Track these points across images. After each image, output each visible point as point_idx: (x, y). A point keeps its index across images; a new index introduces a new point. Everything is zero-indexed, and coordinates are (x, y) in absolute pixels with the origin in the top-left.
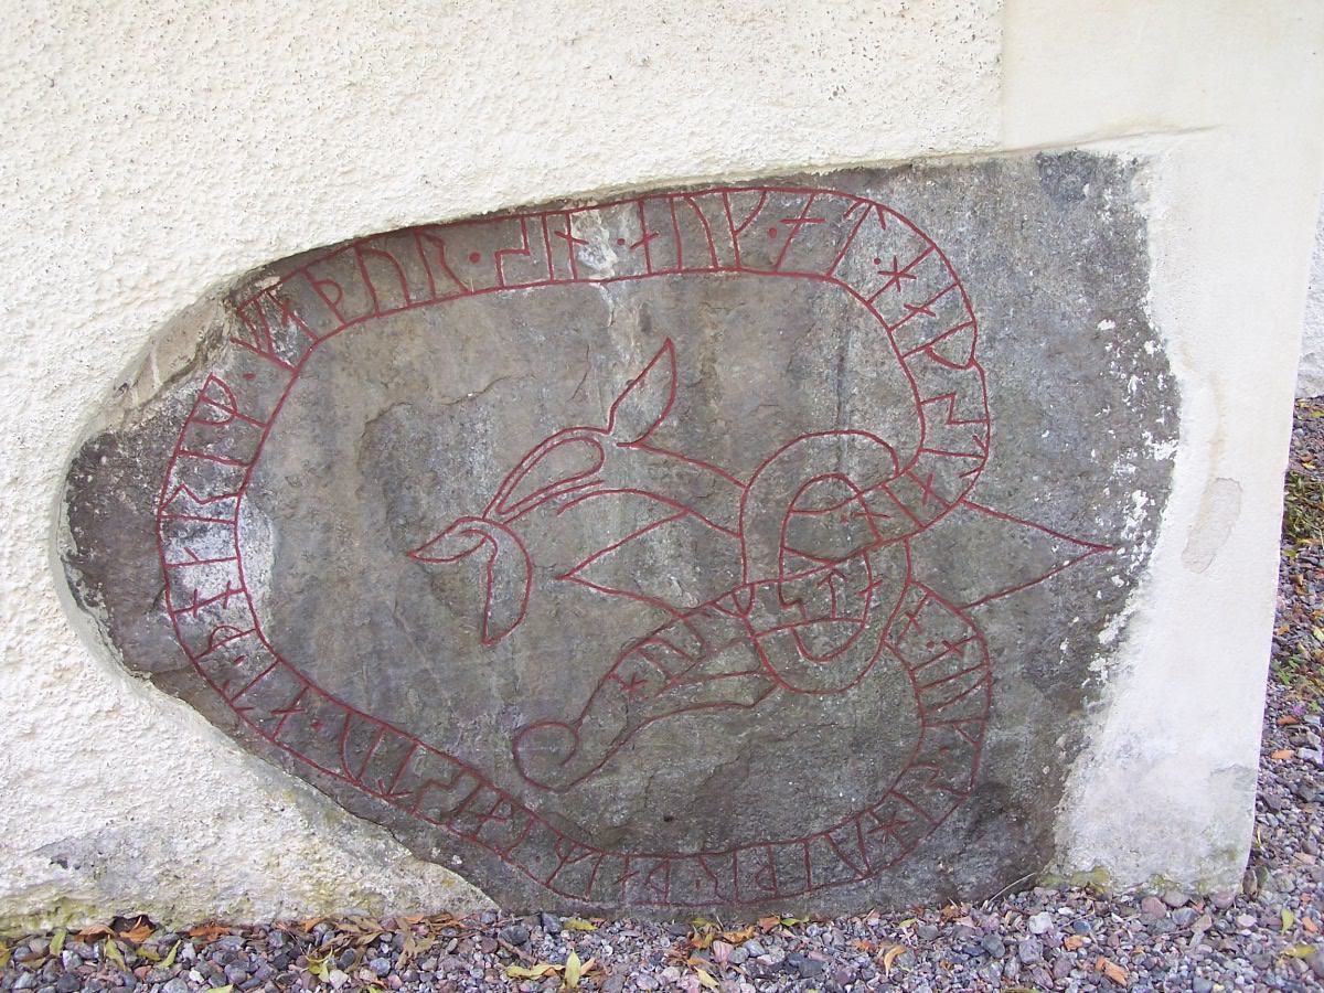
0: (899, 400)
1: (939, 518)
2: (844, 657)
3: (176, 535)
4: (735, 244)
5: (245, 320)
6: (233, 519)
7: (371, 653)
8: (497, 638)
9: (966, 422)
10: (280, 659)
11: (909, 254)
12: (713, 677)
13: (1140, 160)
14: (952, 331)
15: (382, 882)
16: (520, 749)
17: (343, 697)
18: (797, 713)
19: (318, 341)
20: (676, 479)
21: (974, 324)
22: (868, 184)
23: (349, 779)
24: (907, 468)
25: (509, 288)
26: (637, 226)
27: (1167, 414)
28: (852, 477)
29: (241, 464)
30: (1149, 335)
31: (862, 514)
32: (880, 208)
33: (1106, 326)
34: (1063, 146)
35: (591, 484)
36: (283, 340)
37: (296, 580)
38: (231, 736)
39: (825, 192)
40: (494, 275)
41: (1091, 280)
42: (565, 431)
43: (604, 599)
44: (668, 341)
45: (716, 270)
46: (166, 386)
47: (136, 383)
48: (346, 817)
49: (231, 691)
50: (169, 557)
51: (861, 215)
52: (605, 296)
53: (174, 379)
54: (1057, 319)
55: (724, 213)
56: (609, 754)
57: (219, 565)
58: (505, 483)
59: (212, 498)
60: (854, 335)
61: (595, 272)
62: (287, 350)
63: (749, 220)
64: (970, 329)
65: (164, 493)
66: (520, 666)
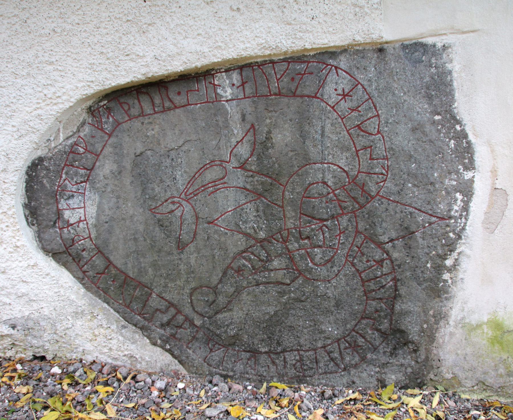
0: (348, 150)
1: (368, 203)
2: (329, 265)
3: (63, 198)
4: (278, 85)
5: (94, 116)
6: (83, 192)
7: (134, 251)
8: (183, 248)
9: (377, 159)
10: (99, 251)
11: (349, 87)
12: (272, 270)
13: (446, 45)
14: (369, 119)
15: (133, 349)
16: (193, 298)
17: (123, 269)
18: (308, 289)
19: (119, 124)
20: (256, 183)
21: (378, 116)
22: (331, 58)
23: (125, 306)
24: (354, 180)
25: (191, 105)
26: (239, 78)
27: (469, 158)
28: (330, 183)
29: (88, 170)
30: (459, 122)
31: (335, 200)
32: (336, 68)
33: (437, 118)
34: (411, 40)
35: (222, 184)
36: (107, 124)
37: (105, 217)
38: (81, 283)
39: (313, 62)
40: (186, 100)
41: (429, 98)
42: (212, 162)
43: (226, 233)
44: (252, 125)
45: (271, 95)
46: (64, 140)
47: (54, 140)
48: (124, 323)
49: (82, 263)
50: (60, 206)
51: (328, 71)
52: (227, 107)
53: (67, 138)
54: (415, 114)
55: (273, 72)
56: (230, 302)
57: (77, 210)
58: (189, 183)
59: (77, 183)
60: (328, 121)
61: (223, 97)
62: (108, 127)
63: (283, 74)
64: (376, 118)
65: (60, 181)
66: (193, 261)
